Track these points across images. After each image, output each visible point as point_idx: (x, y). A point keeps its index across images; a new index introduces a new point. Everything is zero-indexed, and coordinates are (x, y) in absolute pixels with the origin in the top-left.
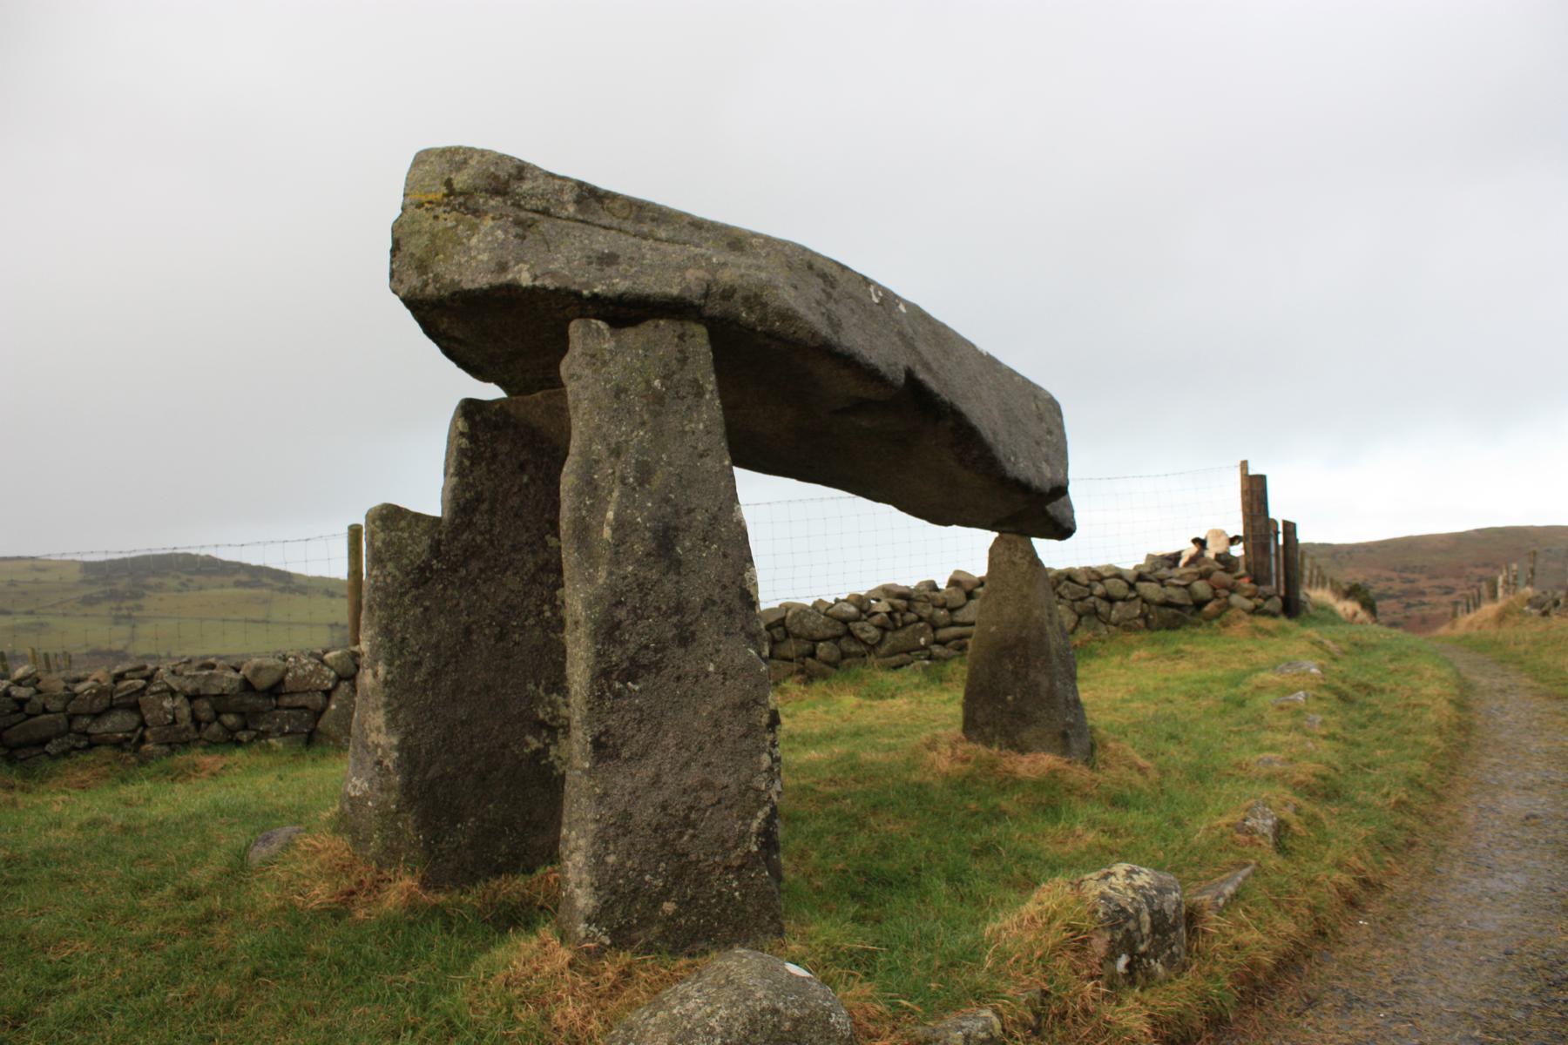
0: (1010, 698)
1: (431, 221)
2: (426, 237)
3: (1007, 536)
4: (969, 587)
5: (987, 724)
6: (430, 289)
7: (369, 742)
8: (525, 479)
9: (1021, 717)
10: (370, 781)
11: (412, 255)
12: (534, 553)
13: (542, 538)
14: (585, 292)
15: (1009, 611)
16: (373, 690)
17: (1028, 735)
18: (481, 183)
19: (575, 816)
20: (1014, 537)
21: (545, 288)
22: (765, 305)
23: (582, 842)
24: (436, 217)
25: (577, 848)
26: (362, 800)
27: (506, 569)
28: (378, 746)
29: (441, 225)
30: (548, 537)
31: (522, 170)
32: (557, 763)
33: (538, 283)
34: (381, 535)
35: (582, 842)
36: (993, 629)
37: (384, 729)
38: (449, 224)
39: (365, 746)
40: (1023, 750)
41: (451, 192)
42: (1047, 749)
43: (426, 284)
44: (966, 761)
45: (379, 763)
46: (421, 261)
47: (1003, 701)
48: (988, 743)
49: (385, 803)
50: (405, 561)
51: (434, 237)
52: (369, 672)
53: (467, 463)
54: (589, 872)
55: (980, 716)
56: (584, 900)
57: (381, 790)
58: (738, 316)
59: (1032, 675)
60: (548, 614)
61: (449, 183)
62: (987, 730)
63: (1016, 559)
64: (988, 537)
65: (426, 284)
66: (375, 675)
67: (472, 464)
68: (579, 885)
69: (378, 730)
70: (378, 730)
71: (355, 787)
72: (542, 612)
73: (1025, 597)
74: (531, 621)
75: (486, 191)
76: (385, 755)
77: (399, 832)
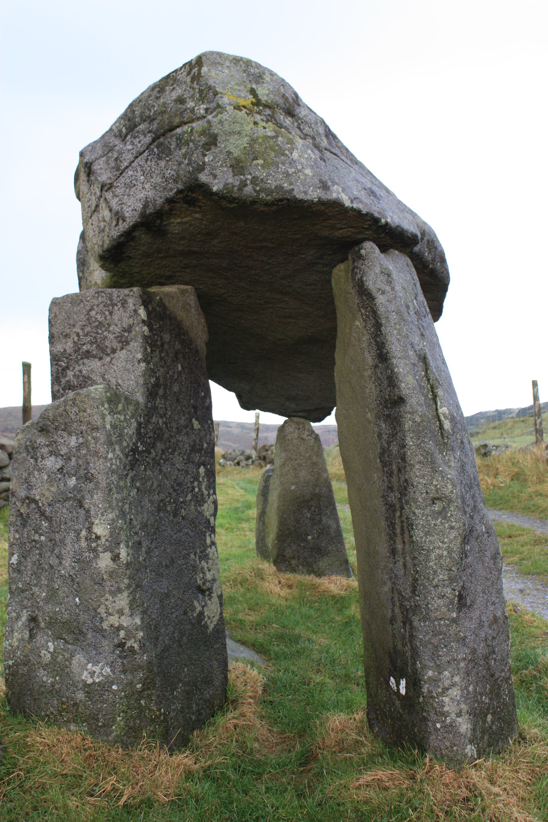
0: (309, 537)
1: (251, 126)
2: (246, 139)
3: (295, 419)
4: (10, 450)
5: (294, 558)
6: (249, 189)
7: (105, 625)
8: (180, 368)
9: (318, 551)
10: (112, 665)
11: (229, 153)
12: (187, 434)
13: (191, 421)
14: (383, 221)
15: (303, 474)
16: (111, 574)
17: (323, 563)
18: (281, 101)
19: (445, 659)
20: (302, 420)
21: (359, 212)
22: (436, 248)
23: (457, 679)
24: (255, 123)
25: (454, 685)
26: (104, 686)
27: (175, 450)
28: (119, 628)
29: (260, 132)
30: (194, 420)
32: (209, 622)
33: (355, 206)
34: (108, 418)
35: (457, 679)
36: (293, 487)
37: (127, 611)
38: (269, 134)
39: (101, 631)
40: (319, 575)
41: (258, 103)
42: (337, 573)
43: (244, 184)
44: (290, 587)
45: (121, 645)
46: (238, 161)
47: (305, 540)
48: (293, 570)
49: (131, 684)
50: (125, 444)
51: (254, 141)
52: (108, 555)
53: (149, 350)
54: (465, 702)
55: (289, 552)
56: (464, 726)
57: (124, 672)
58: (424, 253)
59: (324, 520)
60: (197, 490)
61: (253, 92)
62: (293, 562)
63: (305, 436)
65: (244, 184)
66: (116, 558)
67: (152, 351)
68: (459, 715)
69: (121, 612)
70: (121, 612)
71: (92, 674)
72: (193, 488)
73: (315, 464)
74: (189, 497)
75: (283, 109)
76: (128, 636)
77: (141, 710)
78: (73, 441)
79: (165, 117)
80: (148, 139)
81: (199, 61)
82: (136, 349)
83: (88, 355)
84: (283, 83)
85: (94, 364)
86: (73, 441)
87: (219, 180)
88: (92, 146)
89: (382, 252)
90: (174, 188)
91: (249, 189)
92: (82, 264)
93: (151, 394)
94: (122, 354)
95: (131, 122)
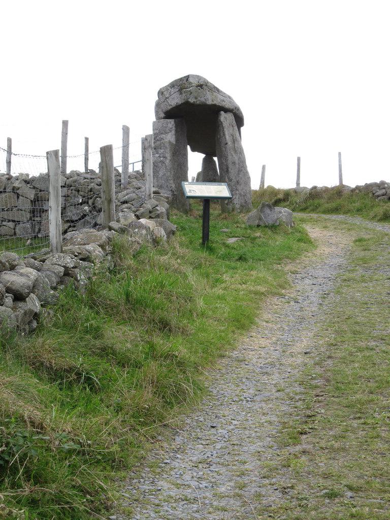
6: (198, 102)
31: (208, 82)
64: (203, 156)
78: (162, 151)
79: (182, 85)
80: (178, 90)
81: (188, 76)
82: (173, 132)
83: (162, 133)
84: (205, 79)
85: (164, 136)
86: (162, 151)
87: (192, 100)
88: (163, 88)
89: (225, 113)
90: (183, 101)
91: (198, 102)
92: (157, 113)
93: (177, 140)
94: (170, 134)
95: (172, 85)
